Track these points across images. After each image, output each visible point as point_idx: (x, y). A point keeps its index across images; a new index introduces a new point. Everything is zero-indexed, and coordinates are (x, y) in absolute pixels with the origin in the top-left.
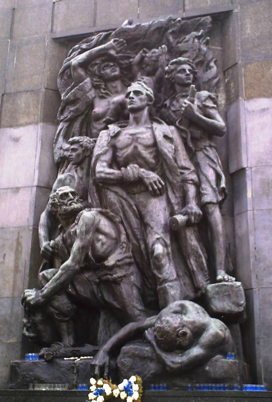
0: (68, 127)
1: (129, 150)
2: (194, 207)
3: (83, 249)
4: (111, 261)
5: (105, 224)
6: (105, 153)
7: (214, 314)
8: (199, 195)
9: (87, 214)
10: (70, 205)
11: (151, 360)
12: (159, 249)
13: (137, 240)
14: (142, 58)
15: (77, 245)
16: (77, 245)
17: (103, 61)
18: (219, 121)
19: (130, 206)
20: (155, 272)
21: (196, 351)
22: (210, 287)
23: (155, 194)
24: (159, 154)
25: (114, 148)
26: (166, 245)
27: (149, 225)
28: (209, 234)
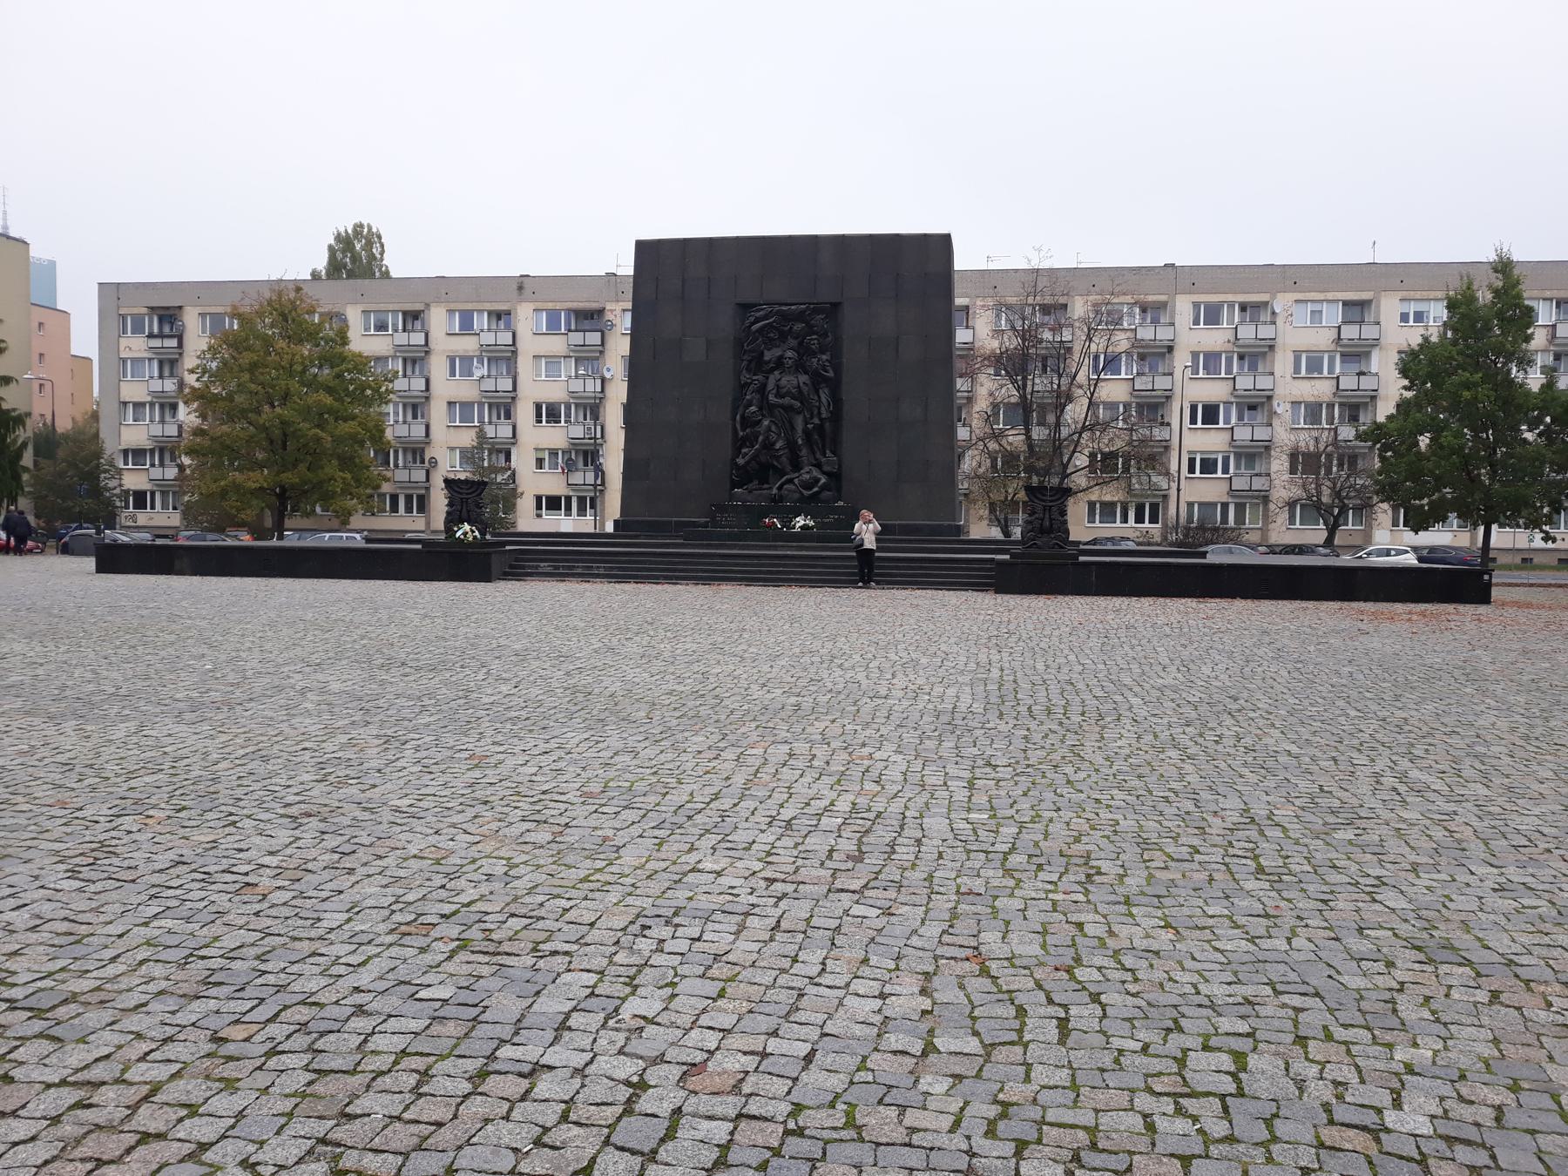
2: (816, 421)
3: (764, 441)
5: (773, 428)
7: (824, 473)
8: (819, 413)
9: (766, 423)
12: (800, 442)
15: (761, 438)
16: (761, 438)
18: (831, 374)
21: (816, 489)
22: (823, 460)
23: (799, 413)
24: (800, 391)
25: (778, 387)
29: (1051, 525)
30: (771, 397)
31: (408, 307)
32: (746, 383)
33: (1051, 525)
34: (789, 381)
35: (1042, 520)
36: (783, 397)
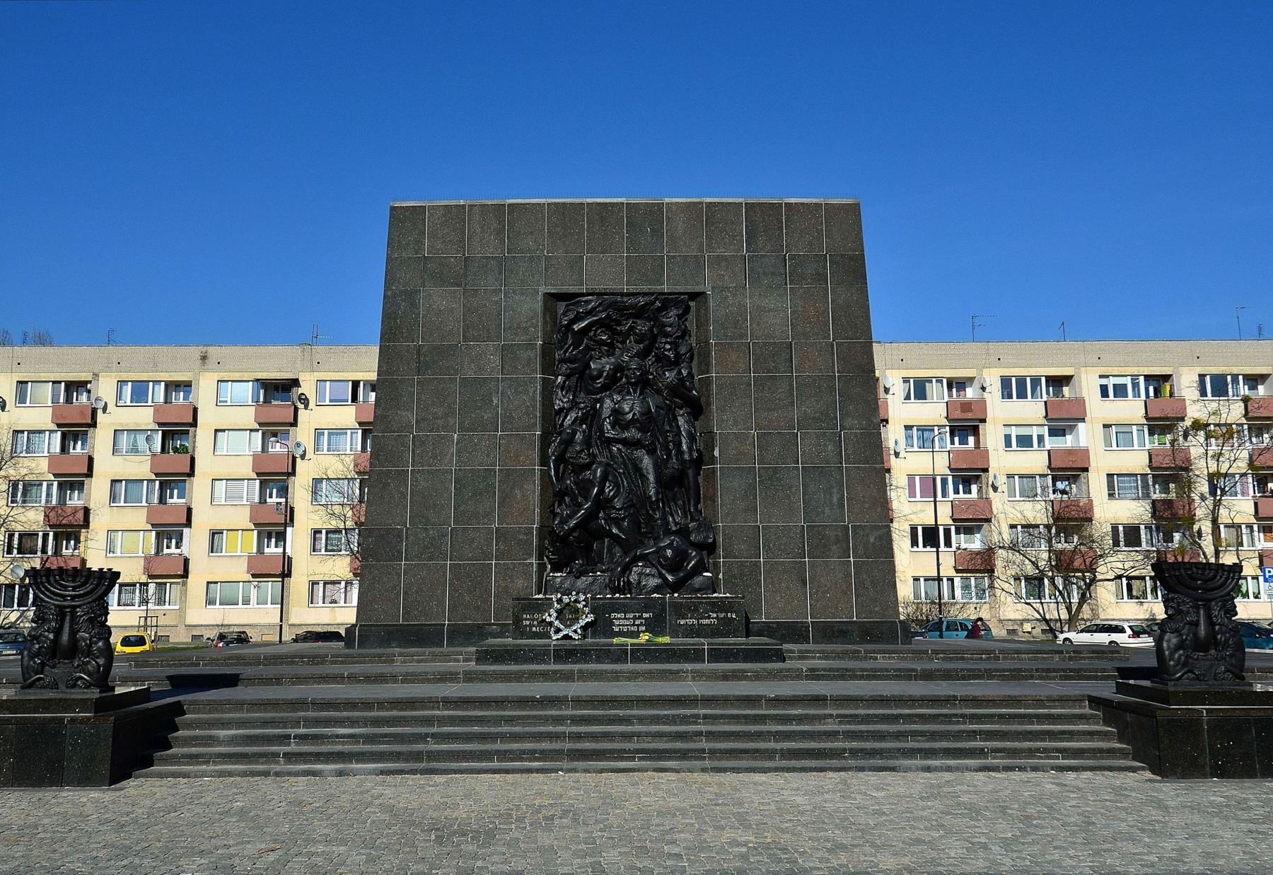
0: (564, 382)
1: (630, 416)
4: (618, 504)
6: (609, 417)
8: (680, 452)
10: (586, 459)
11: (653, 576)
13: (635, 486)
14: (631, 328)
17: (600, 328)
19: (629, 459)
20: (651, 512)
26: (657, 493)
27: (645, 476)
28: (686, 483)
29: (1214, 634)
30: (607, 426)
32: (561, 410)
33: (1212, 634)
34: (631, 406)
35: (1197, 624)
36: (626, 426)
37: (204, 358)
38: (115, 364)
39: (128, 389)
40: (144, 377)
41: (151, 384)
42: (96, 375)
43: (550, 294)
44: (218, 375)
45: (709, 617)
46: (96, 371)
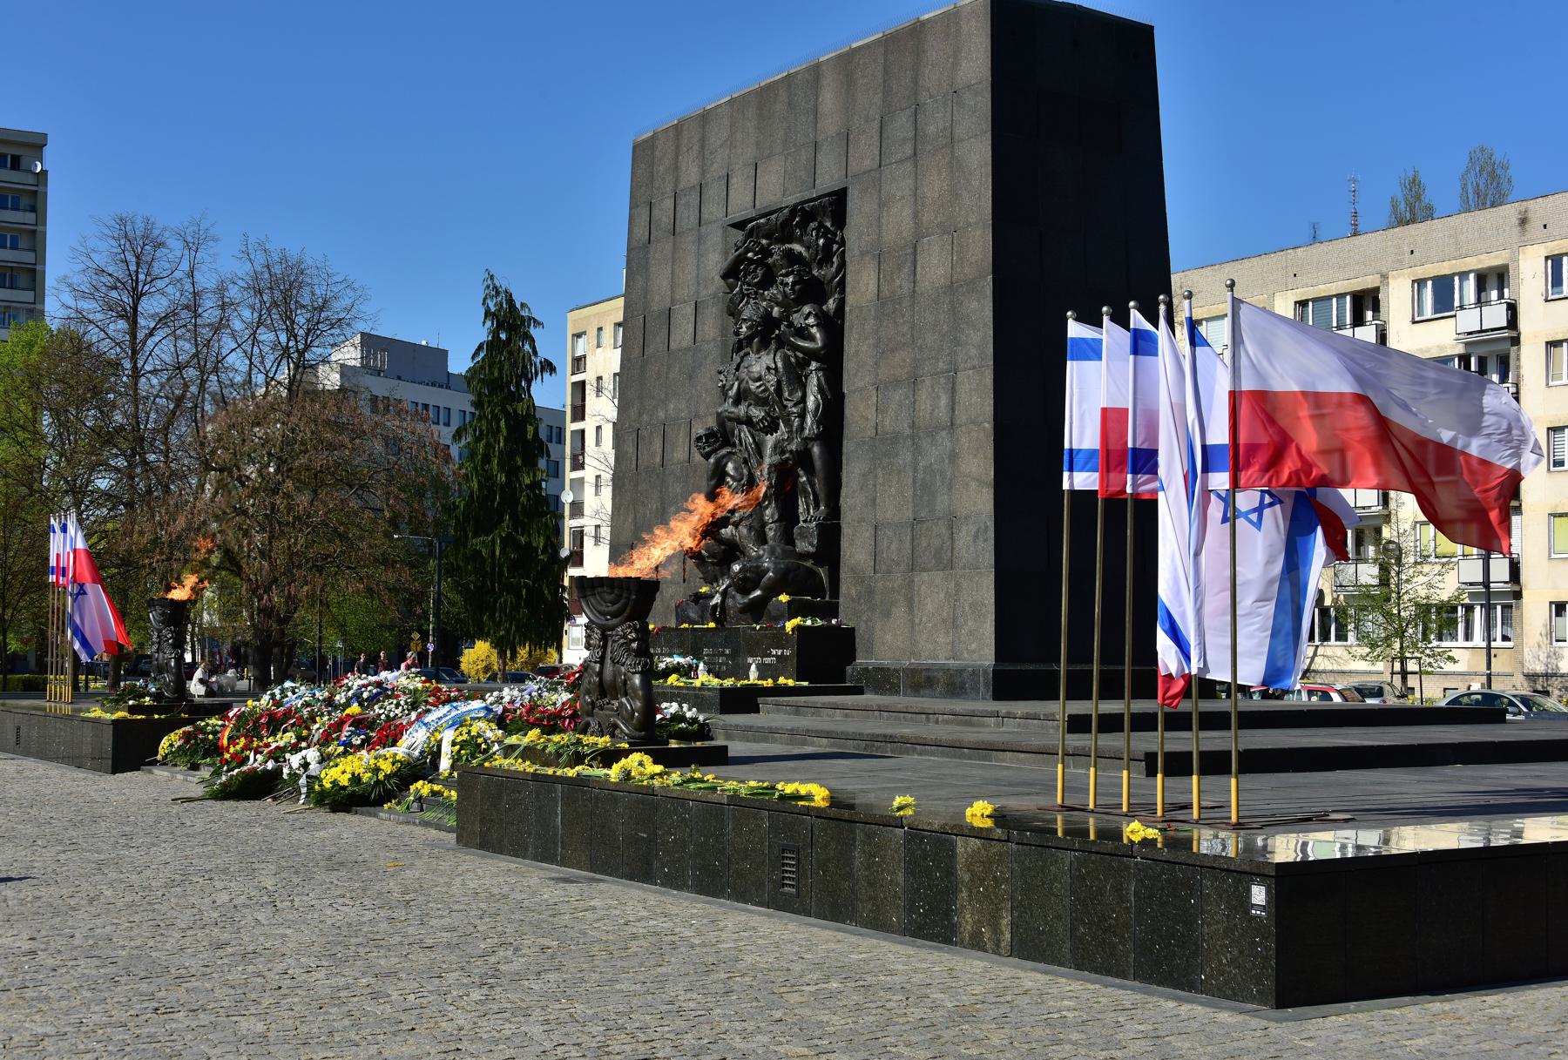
8: (802, 428)
31: (1359, 284)
37: (1523, 222)
38: (1407, 255)
39: (1428, 293)
40: (1445, 269)
41: (1456, 278)
42: (1385, 277)
43: (731, 226)
44: (1545, 248)
45: (769, 655)
46: (1384, 271)
